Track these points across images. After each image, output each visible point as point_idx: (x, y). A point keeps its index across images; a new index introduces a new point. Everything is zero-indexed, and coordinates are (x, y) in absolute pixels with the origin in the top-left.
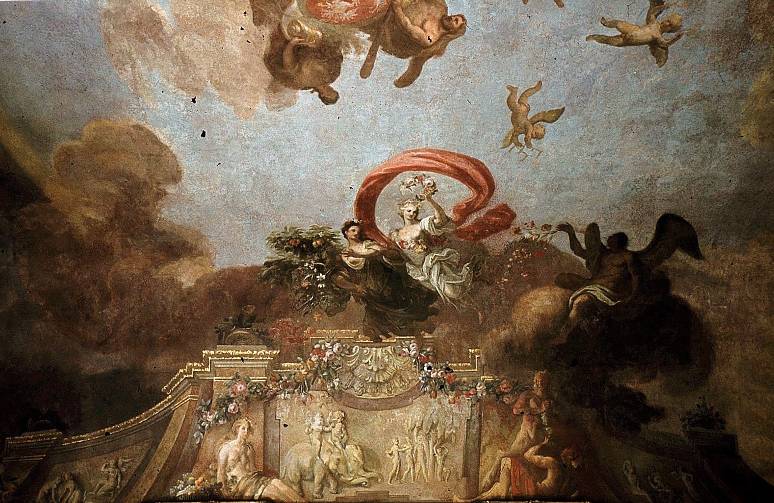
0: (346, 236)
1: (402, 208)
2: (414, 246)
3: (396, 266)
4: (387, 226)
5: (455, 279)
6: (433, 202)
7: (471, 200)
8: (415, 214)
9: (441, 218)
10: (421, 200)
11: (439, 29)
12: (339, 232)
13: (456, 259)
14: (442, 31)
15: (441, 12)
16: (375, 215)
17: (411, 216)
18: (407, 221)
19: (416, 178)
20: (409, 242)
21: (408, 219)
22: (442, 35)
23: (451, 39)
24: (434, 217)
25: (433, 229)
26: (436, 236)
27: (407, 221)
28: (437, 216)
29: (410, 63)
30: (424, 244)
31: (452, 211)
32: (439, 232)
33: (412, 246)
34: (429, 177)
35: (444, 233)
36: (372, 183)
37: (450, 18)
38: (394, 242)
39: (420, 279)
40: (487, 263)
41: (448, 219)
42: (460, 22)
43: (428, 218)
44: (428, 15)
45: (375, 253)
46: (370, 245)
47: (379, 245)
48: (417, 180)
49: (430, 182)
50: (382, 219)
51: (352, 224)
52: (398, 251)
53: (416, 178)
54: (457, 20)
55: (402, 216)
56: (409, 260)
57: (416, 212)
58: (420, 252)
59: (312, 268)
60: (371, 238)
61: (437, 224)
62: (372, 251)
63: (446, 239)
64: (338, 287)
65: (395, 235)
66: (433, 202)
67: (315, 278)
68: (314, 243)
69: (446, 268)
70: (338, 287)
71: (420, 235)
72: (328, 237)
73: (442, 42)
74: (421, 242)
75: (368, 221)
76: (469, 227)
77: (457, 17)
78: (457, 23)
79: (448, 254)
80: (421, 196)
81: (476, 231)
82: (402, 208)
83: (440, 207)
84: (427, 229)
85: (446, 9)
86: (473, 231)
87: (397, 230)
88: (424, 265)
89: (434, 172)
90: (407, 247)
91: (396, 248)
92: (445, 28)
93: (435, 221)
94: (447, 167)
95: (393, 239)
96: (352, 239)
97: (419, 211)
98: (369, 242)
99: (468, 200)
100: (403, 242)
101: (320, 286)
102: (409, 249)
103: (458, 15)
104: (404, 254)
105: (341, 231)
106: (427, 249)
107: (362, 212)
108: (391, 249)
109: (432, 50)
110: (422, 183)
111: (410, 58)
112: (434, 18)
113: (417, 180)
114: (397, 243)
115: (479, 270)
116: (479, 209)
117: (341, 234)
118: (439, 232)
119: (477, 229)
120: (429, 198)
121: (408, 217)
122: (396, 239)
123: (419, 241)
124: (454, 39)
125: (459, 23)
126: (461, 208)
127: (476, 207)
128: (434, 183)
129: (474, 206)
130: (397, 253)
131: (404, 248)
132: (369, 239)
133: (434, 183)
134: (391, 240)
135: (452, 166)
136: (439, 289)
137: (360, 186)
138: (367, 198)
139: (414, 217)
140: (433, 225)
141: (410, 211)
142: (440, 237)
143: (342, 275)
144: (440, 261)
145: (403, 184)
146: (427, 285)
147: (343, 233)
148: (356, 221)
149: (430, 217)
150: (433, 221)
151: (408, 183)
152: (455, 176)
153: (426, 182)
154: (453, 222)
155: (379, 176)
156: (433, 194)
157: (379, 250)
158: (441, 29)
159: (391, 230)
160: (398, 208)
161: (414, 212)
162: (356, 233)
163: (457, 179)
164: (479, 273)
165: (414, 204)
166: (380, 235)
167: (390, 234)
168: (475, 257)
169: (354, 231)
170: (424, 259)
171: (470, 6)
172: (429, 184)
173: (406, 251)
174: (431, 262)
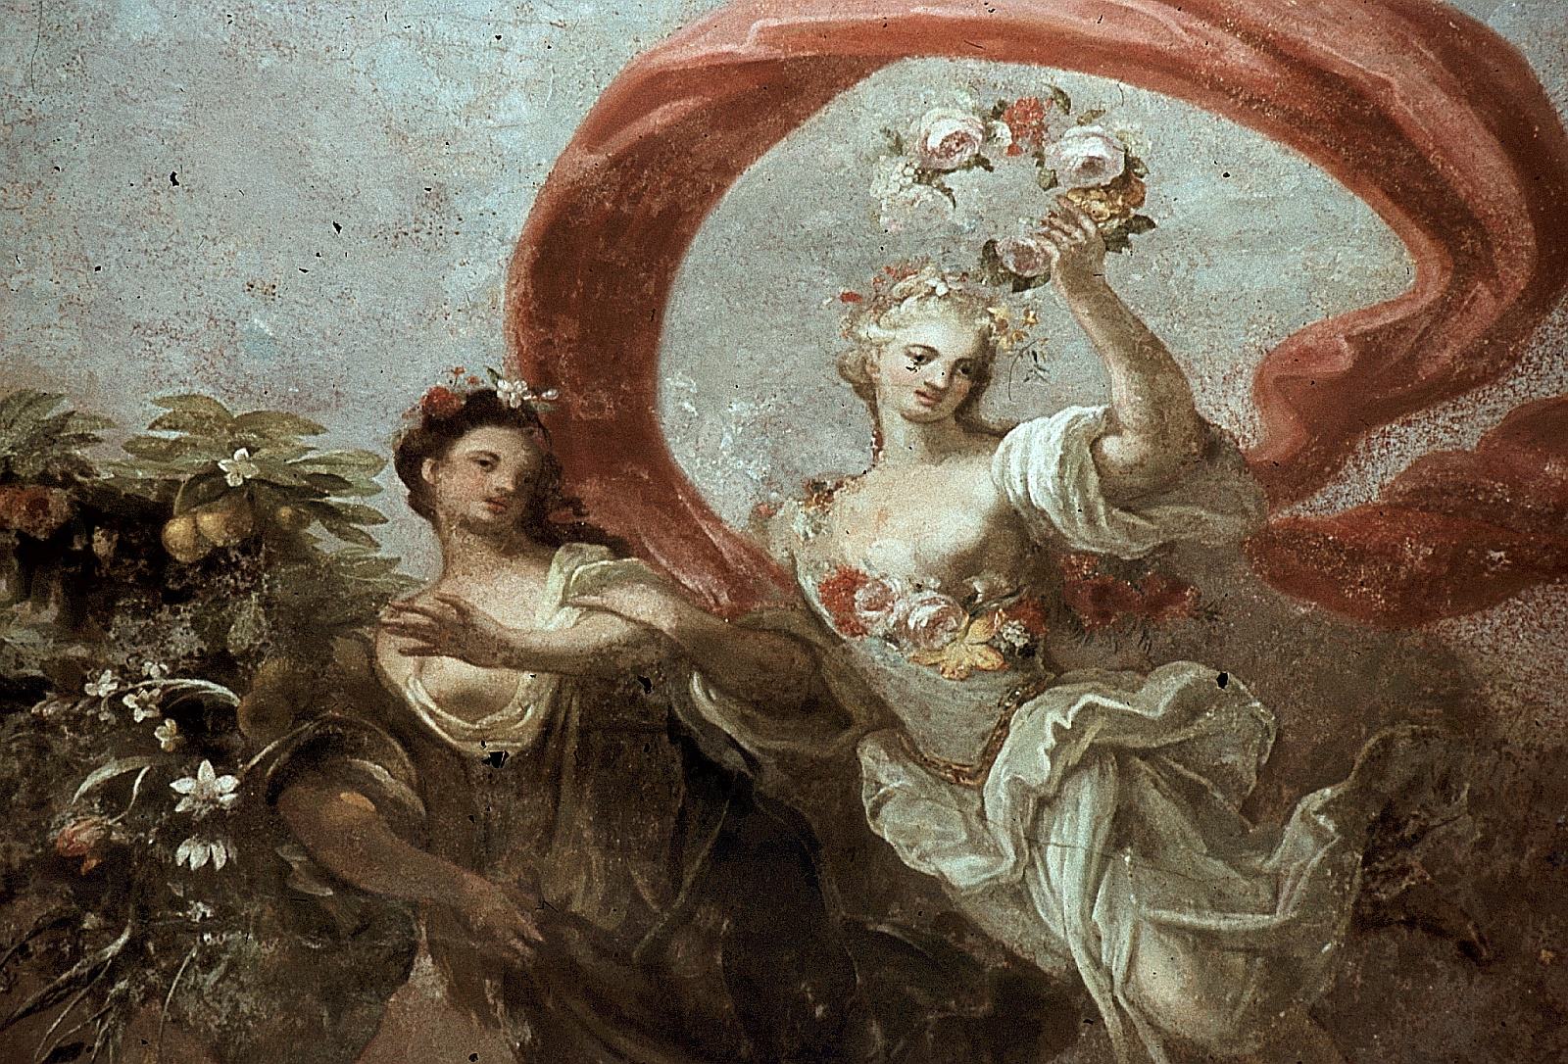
0: (422, 501)
1: (870, 330)
2: (935, 623)
3: (785, 760)
4: (738, 451)
5: (1221, 902)
6: (1109, 309)
7: (1399, 314)
8: (962, 383)
9: (1158, 431)
10: (1022, 284)
12: (378, 465)
13: (1243, 747)
16: (664, 365)
17: (934, 395)
18: (898, 431)
19: (997, 114)
20: (896, 585)
21: (910, 418)
24: (1110, 416)
25: (1089, 510)
26: (1112, 561)
27: (898, 431)
28: (1127, 415)
30: (1012, 613)
31: (1244, 385)
32: (1131, 532)
33: (922, 615)
34: (1096, 114)
35: (1169, 547)
36: (658, 119)
38: (787, 579)
39: (961, 870)
40: (1475, 801)
41: (1211, 444)
43: (1063, 418)
45: (634, 643)
46: (603, 581)
47: (670, 586)
48: (1003, 130)
49: (1097, 149)
50: (709, 397)
51: (482, 408)
52: (808, 646)
53: (997, 114)
55: (867, 390)
56: (886, 723)
57: (977, 370)
58: (974, 671)
59: (139, 716)
60: (612, 529)
61: (1130, 469)
62: (606, 630)
63: (1177, 587)
64: (329, 878)
65: (799, 526)
66: (1109, 309)
67: (158, 794)
68: (177, 530)
69: (1161, 810)
70: (329, 878)
71: (983, 547)
72: (289, 493)
74: (992, 593)
75: (604, 397)
76: (1364, 517)
79: (1189, 707)
80: (1023, 253)
81: (1416, 554)
82: (870, 330)
83: (1154, 341)
84: (1040, 500)
86: (1390, 552)
87: (819, 492)
88: (999, 772)
89: (1139, 82)
90: (880, 622)
91: (796, 622)
93: (1111, 446)
94: (1239, 55)
95: (778, 554)
96: (468, 525)
97: (996, 366)
98: (593, 561)
99: (1373, 312)
100: (850, 580)
101: (192, 854)
102: (889, 637)
104: (849, 672)
105: (390, 455)
106: (1028, 652)
107: (569, 329)
108: (756, 627)
110: (1040, 156)
113: (1003, 130)
114: (808, 583)
115: (1408, 844)
116: (1450, 387)
117: (392, 486)
118: (1131, 532)
119: (1424, 539)
120: (1081, 276)
121: (912, 403)
122: (802, 557)
123: (978, 586)
126: (1321, 370)
127: (1428, 370)
128: (1131, 163)
129: (1410, 360)
130: (801, 660)
131: (859, 630)
132: (595, 536)
133: (1131, 163)
134: (760, 558)
135: (1279, 50)
136: (1097, 963)
137: (566, 136)
138: (614, 226)
139: (951, 402)
140: (1093, 478)
141: (925, 356)
142: (1138, 564)
143: (367, 786)
144: (1122, 754)
145: (898, 148)
146: (1004, 924)
147: (408, 462)
148: (511, 391)
149: (1075, 410)
150: (1094, 444)
151: (934, 143)
152: (1293, 130)
153: (1075, 147)
154: (1244, 464)
155: (718, 71)
156: (1117, 242)
157: (665, 623)
159: (768, 481)
160: (840, 322)
161: (960, 366)
162: (502, 480)
163: (1310, 149)
164: (1405, 871)
165: (965, 303)
166: (679, 514)
167: (762, 516)
168: (1387, 743)
169: (489, 462)
170: (1004, 725)
172: (1092, 165)
173: (869, 651)
174: (1053, 754)
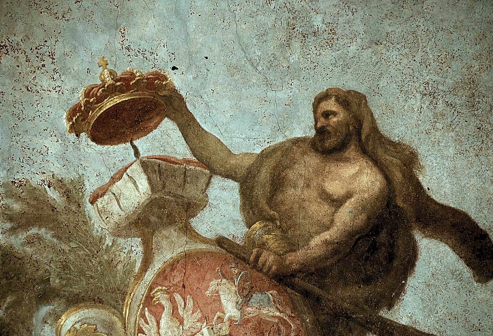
11: (347, 160)
14: (351, 152)
15: (304, 153)
22: (364, 152)
23: (375, 129)
29: (431, 237)
37: (321, 132)
42: (331, 105)
44: (308, 186)
54: (327, 115)
73: (380, 151)
77: (320, 111)
78: (335, 114)
85: (297, 141)
92: (342, 147)
103: (315, 112)
109: (398, 176)
111: (418, 236)
112: (319, 172)
124: (373, 121)
125: (334, 109)
158: (346, 154)
171: (295, 82)
